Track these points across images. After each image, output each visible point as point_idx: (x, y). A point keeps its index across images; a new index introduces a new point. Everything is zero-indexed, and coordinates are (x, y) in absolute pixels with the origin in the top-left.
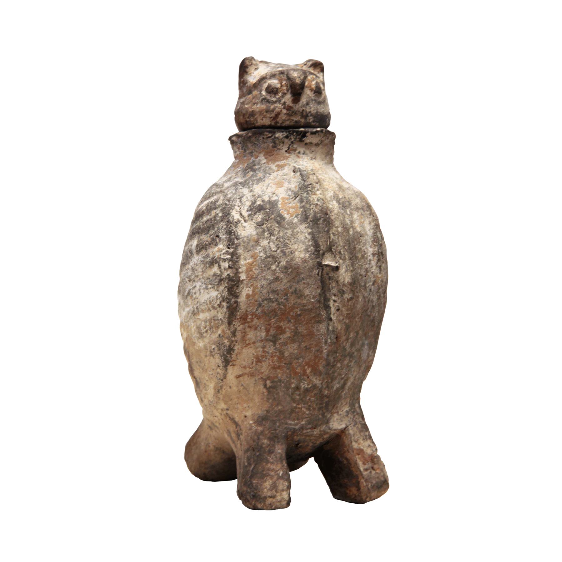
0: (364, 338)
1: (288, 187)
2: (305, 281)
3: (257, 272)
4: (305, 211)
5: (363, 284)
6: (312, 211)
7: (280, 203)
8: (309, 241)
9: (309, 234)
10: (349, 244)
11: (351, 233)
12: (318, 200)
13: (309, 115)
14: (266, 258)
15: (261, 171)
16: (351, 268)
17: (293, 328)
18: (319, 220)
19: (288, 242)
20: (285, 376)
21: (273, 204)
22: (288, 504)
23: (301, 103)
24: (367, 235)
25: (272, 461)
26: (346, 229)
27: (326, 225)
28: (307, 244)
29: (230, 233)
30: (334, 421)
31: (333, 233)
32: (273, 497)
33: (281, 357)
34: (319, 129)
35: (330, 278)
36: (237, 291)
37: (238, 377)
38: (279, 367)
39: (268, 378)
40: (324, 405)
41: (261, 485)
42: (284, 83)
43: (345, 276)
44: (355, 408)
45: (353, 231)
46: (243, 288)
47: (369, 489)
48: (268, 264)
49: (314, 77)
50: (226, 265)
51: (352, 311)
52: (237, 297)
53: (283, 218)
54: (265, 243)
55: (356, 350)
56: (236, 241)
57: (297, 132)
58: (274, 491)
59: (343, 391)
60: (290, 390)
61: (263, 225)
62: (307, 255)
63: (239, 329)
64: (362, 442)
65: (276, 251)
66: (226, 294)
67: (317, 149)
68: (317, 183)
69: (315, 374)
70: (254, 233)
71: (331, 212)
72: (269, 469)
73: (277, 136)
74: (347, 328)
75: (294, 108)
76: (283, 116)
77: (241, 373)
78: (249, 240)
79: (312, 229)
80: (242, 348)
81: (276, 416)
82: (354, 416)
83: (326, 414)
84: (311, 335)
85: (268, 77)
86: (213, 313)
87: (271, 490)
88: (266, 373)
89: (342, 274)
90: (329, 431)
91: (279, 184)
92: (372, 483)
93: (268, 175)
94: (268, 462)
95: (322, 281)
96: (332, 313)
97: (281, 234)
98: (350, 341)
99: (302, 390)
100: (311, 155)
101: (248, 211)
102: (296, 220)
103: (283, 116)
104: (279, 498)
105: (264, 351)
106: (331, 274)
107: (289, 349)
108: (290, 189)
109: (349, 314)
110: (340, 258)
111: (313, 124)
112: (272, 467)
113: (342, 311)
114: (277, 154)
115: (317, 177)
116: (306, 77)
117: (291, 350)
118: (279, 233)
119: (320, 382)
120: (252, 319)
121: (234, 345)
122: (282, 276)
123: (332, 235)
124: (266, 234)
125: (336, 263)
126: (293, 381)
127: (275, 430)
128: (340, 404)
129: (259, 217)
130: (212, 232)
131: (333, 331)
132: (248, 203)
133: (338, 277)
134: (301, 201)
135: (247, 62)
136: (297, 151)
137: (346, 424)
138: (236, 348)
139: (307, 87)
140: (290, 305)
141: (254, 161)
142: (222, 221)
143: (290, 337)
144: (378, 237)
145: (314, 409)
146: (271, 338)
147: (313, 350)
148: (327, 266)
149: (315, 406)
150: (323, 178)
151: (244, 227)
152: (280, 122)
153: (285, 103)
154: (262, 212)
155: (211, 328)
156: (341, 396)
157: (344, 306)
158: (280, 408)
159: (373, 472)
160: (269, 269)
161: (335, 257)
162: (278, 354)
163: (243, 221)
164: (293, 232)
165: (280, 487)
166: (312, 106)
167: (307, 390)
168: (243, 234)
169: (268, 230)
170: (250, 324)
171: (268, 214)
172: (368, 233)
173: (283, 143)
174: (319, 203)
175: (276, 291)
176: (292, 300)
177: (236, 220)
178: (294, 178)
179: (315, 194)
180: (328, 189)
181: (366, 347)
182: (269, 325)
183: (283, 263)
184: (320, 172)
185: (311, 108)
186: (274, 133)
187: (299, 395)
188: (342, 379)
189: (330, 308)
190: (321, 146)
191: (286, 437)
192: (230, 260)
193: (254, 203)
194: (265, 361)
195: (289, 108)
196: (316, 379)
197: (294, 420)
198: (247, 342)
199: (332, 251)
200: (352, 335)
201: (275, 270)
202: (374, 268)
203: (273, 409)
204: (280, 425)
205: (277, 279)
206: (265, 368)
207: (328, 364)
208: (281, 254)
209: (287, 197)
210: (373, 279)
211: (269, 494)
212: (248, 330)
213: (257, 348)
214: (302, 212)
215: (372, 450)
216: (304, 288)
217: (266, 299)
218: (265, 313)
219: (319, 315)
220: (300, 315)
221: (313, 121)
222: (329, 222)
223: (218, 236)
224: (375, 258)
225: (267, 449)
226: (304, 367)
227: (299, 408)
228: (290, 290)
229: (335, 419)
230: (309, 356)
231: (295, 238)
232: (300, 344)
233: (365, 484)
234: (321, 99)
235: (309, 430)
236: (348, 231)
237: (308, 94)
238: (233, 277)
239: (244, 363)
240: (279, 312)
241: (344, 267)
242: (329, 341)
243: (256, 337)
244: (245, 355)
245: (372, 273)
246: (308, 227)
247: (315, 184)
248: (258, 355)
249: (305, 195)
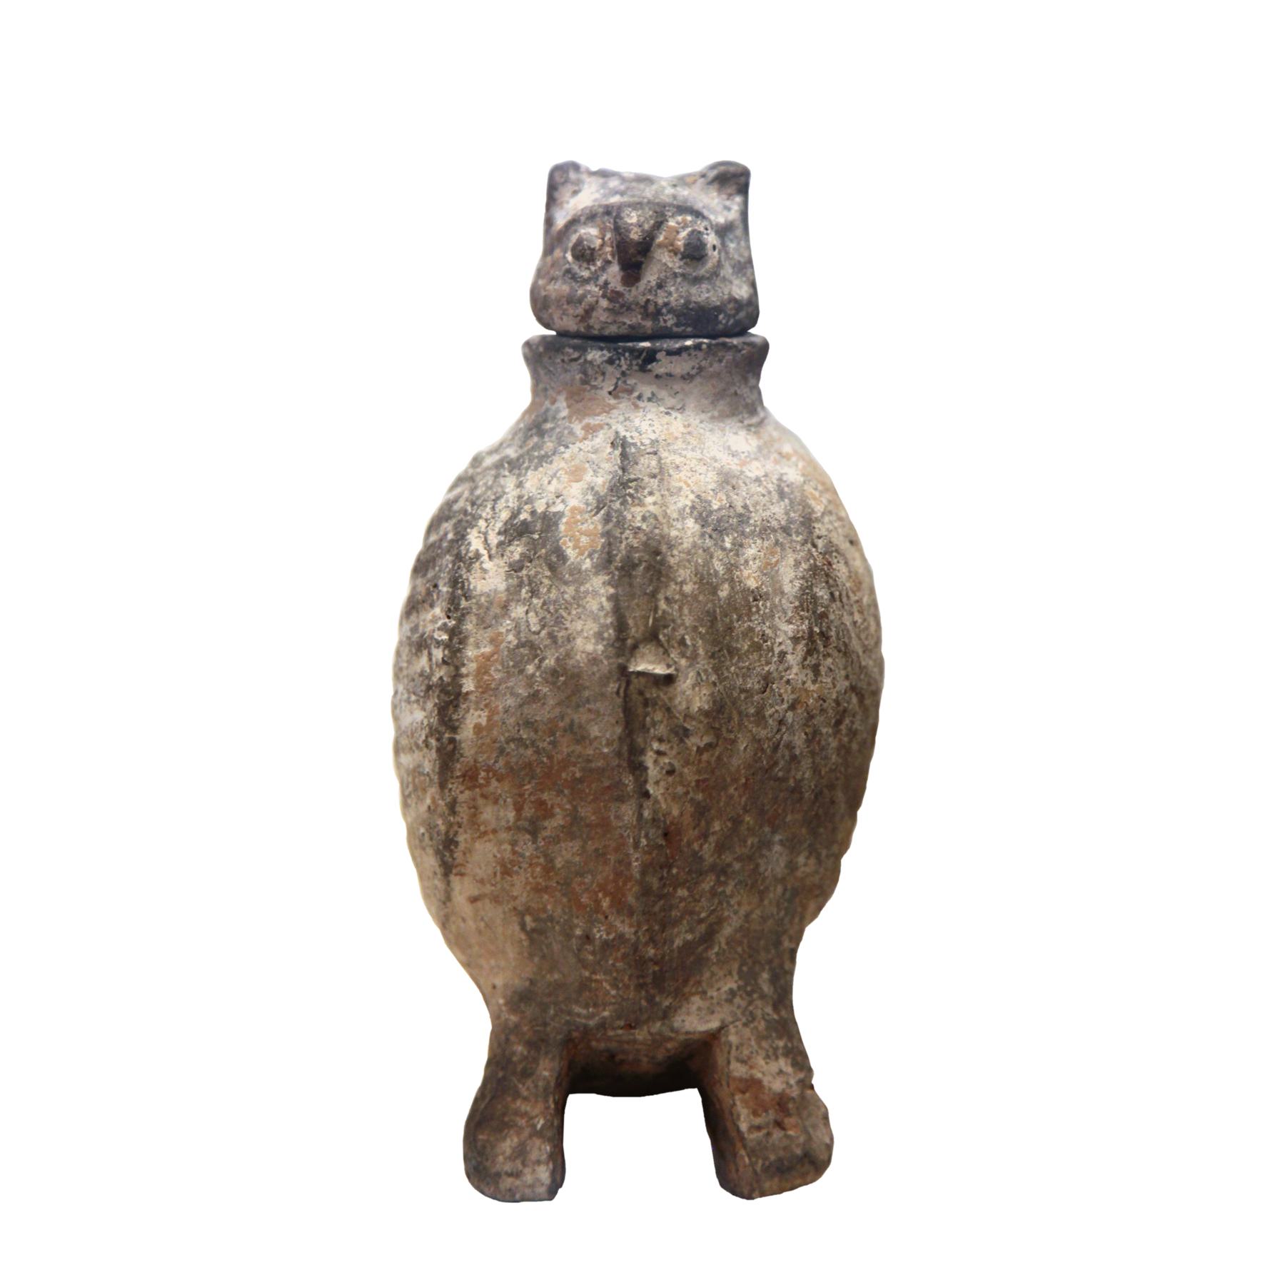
0: (767, 829)
1: (589, 484)
2: (591, 706)
3: (498, 676)
4: (610, 544)
5: (752, 711)
6: (623, 546)
7: (564, 520)
8: (606, 615)
9: (610, 598)
10: (713, 621)
11: (724, 592)
12: (644, 519)
13: (664, 311)
14: (517, 647)
15: (554, 438)
16: (714, 678)
17: (568, 807)
18: (634, 566)
19: (564, 614)
20: (559, 911)
21: (549, 521)
22: (551, 1194)
23: (642, 285)
24: (782, 593)
25: (525, 1093)
26: (707, 583)
27: (651, 580)
28: (602, 621)
29: (455, 582)
30: (688, 1014)
31: (667, 599)
32: (517, 1175)
33: (549, 869)
34: (689, 343)
35: (646, 703)
36: (455, 717)
37: (474, 900)
38: (546, 889)
39: (528, 910)
40: (649, 980)
41: (493, 1147)
42: (608, 236)
43: (692, 694)
44: (757, 984)
45: (733, 588)
46: (467, 711)
47: (755, 1172)
48: (521, 661)
49: (689, 218)
50: (438, 654)
51: (713, 772)
52: (454, 729)
53: (562, 557)
54: (518, 611)
55: (738, 859)
56: (464, 603)
57: (632, 351)
58: (518, 1162)
59: (710, 947)
60: (574, 941)
61: (521, 569)
62: (600, 647)
63: (462, 798)
64: (762, 1062)
65: (538, 633)
66: (434, 720)
67: (687, 387)
68: (654, 476)
69: (618, 912)
70: (502, 586)
71: (671, 547)
72: (517, 1113)
73: (589, 357)
74: (701, 812)
75: (627, 296)
76: (647, 303)
77: (476, 893)
78: (491, 603)
79: (616, 587)
80: (474, 840)
81: (550, 995)
82: (750, 1003)
83: (657, 999)
84: (605, 825)
85: (583, 219)
86: (417, 756)
87: (512, 1158)
88: (523, 899)
89: (684, 693)
90: (673, 1035)
91: (576, 474)
92: (766, 1158)
93: (562, 449)
94: (517, 1095)
95: (627, 710)
96: (651, 781)
97: (553, 595)
98: (712, 839)
99: (597, 943)
100: (671, 401)
101: (499, 533)
102: (587, 564)
103: (647, 303)
104: (528, 1178)
105: (514, 852)
106: (652, 693)
107: (564, 852)
108: (592, 488)
109: (704, 781)
110: (683, 655)
111: (675, 329)
112: (525, 1107)
113: (681, 775)
114: (590, 400)
115: (660, 459)
116: (658, 225)
117: (567, 856)
118: (549, 591)
119: (633, 930)
120: (488, 780)
121: (456, 833)
122: (545, 690)
123: (663, 605)
124: (524, 591)
125: (669, 666)
126: (576, 921)
127: (545, 1024)
128: (707, 975)
129: (517, 550)
130: (430, 574)
131: (654, 820)
132: (505, 515)
133: (671, 699)
134: (607, 519)
135: (557, 178)
136: (636, 394)
137: (723, 1021)
138: (461, 838)
139: (660, 246)
140: (560, 757)
141: (547, 410)
142: (449, 551)
143: (563, 827)
144: (814, 597)
145: (627, 987)
146: (526, 824)
147: (612, 858)
148: (640, 674)
149: (626, 978)
150: (678, 460)
151: (485, 571)
152: (597, 326)
153: (606, 283)
154: (524, 539)
155: (415, 789)
156: (708, 959)
157: (687, 763)
158: (556, 976)
159: (777, 1134)
160: (521, 671)
161: (666, 652)
162: (542, 860)
163: (486, 558)
164: (577, 591)
165: (534, 1155)
166: (672, 289)
167: (606, 945)
168: (479, 588)
169: (530, 584)
170: (485, 789)
171: (534, 546)
172: (787, 588)
173: (603, 374)
174: (644, 527)
175: (532, 723)
176: (566, 747)
177: (470, 555)
178: (608, 460)
179: (641, 504)
180: (680, 489)
181: (777, 848)
182: (521, 795)
183: (550, 662)
184: (679, 445)
185: (670, 294)
186: (583, 350)
187: (593, 953)
188: (701, 921)
189: (646, 769)
190: (698, 380)
191: (568, 1042)
192: (447, 645)
193: (514, 515)
194: (517, 873)
195: (614, 297)
196: (623, 922)
197: (587, 1006)
198: (482, 828)
199: (658, 641)
200: (717, 826)
201: (533, 675)
202: (795, 670)
203: (544, 977)
204: (556, 1015)
205: (535, 697)
206: (519, 887)
207: (646, 892)
208: (548, 642)
209: (582, 506)
210: (789, 697)
211: (508, 1167)
212: (481, 802)
213: (500, 843)
214: (603, 546)
215: (787, 1083)
216: (589, 721)
217: (513, 740)
218: (512, 769)
219: (619, 784)
220: (581, 781)
221: (677, 325)
222: (660, 572)
223: (436, 586)
224: (801, 647)
225: (519, 1068)
226: (596, 893)
227: (596, 981)
228: (561, 724)
229: (694, 1008)
230: (605, 872)
231: (579, 606)
232: (585, 842)
233: (747, 1159)
234: (702, 271)
235: (620, 1032)
236: (714, 590)
237: (664, 260)
238: (449, 684)
239: (480, 873)
240: (538, 770)
241: (692, 674)
242: (644, 842)
243: (498, 819)
244: (482, 855)
245: (788, 682)
246: (609, 584)
247: (646, 479)
248: (503, 859)
249: (617, 505)
